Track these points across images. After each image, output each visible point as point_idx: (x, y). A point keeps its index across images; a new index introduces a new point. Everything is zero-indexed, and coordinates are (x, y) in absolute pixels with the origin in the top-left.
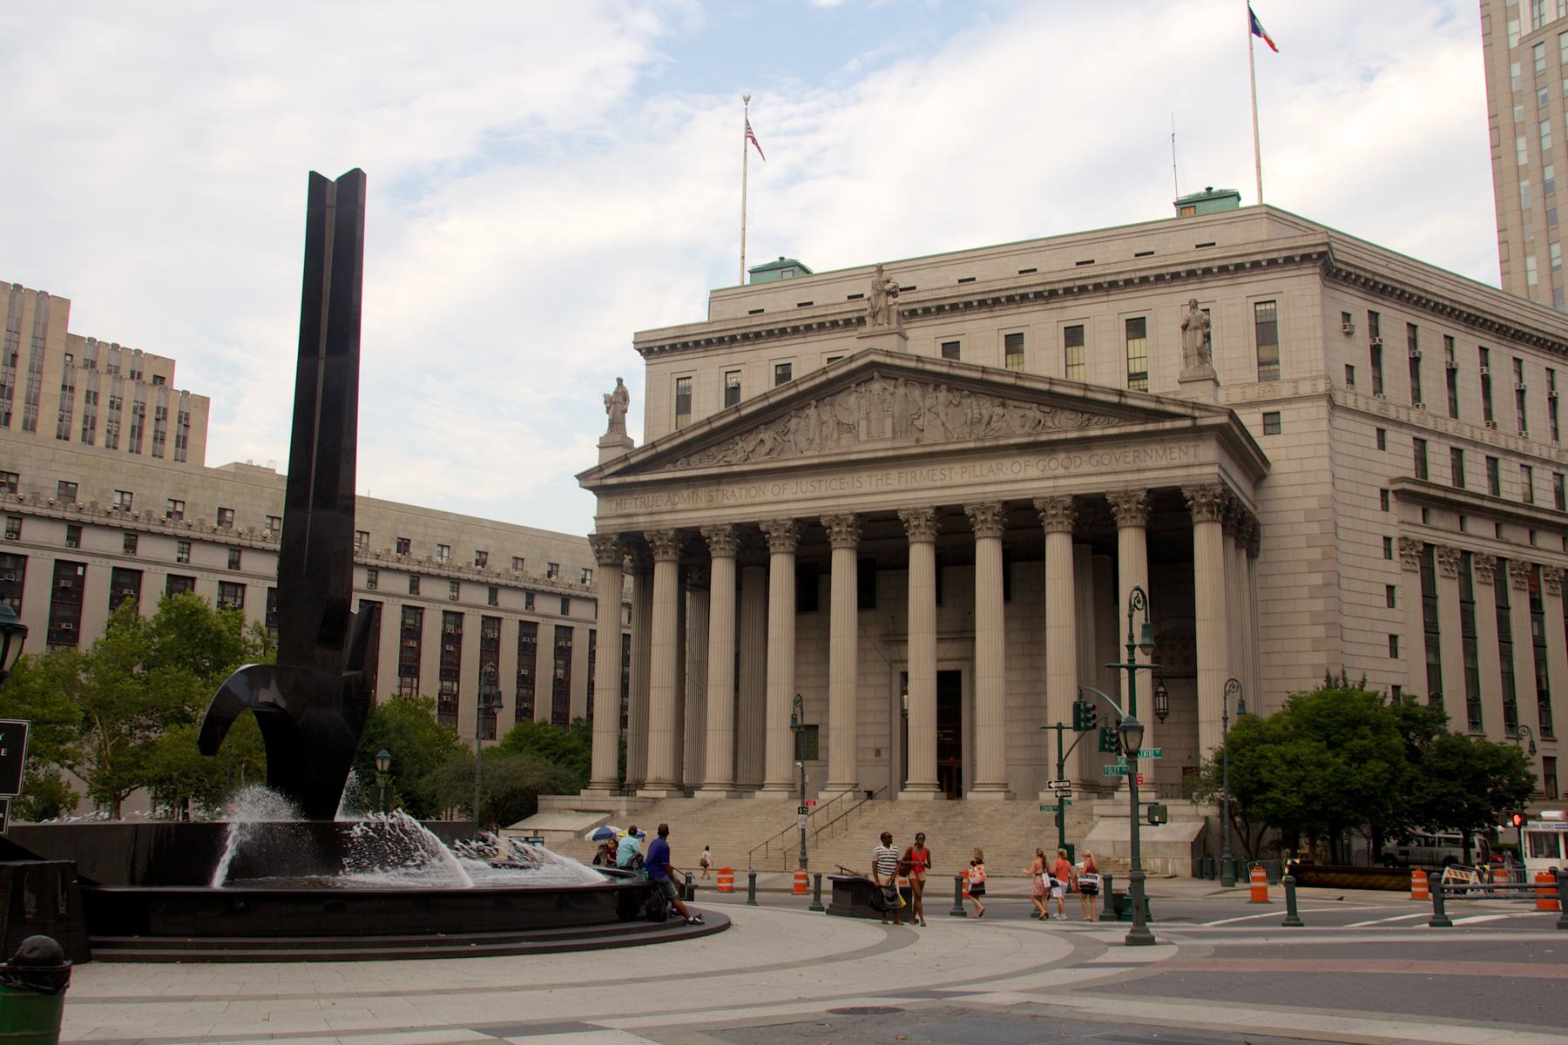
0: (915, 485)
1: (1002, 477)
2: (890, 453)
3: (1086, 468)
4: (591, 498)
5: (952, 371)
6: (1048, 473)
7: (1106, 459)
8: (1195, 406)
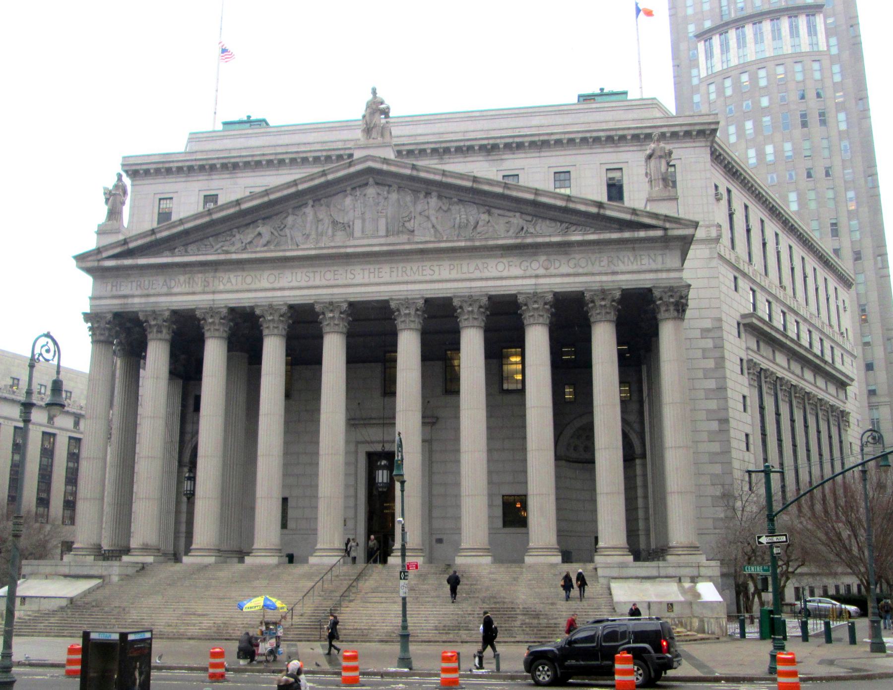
0: (406, 278)
1: (486, 274)
2: (385, 248)
3: (564, 269)
4: (87, 281)
5: (445, 180)
6: (530, 272)
7: (583, 263)
8: (667, 218)
